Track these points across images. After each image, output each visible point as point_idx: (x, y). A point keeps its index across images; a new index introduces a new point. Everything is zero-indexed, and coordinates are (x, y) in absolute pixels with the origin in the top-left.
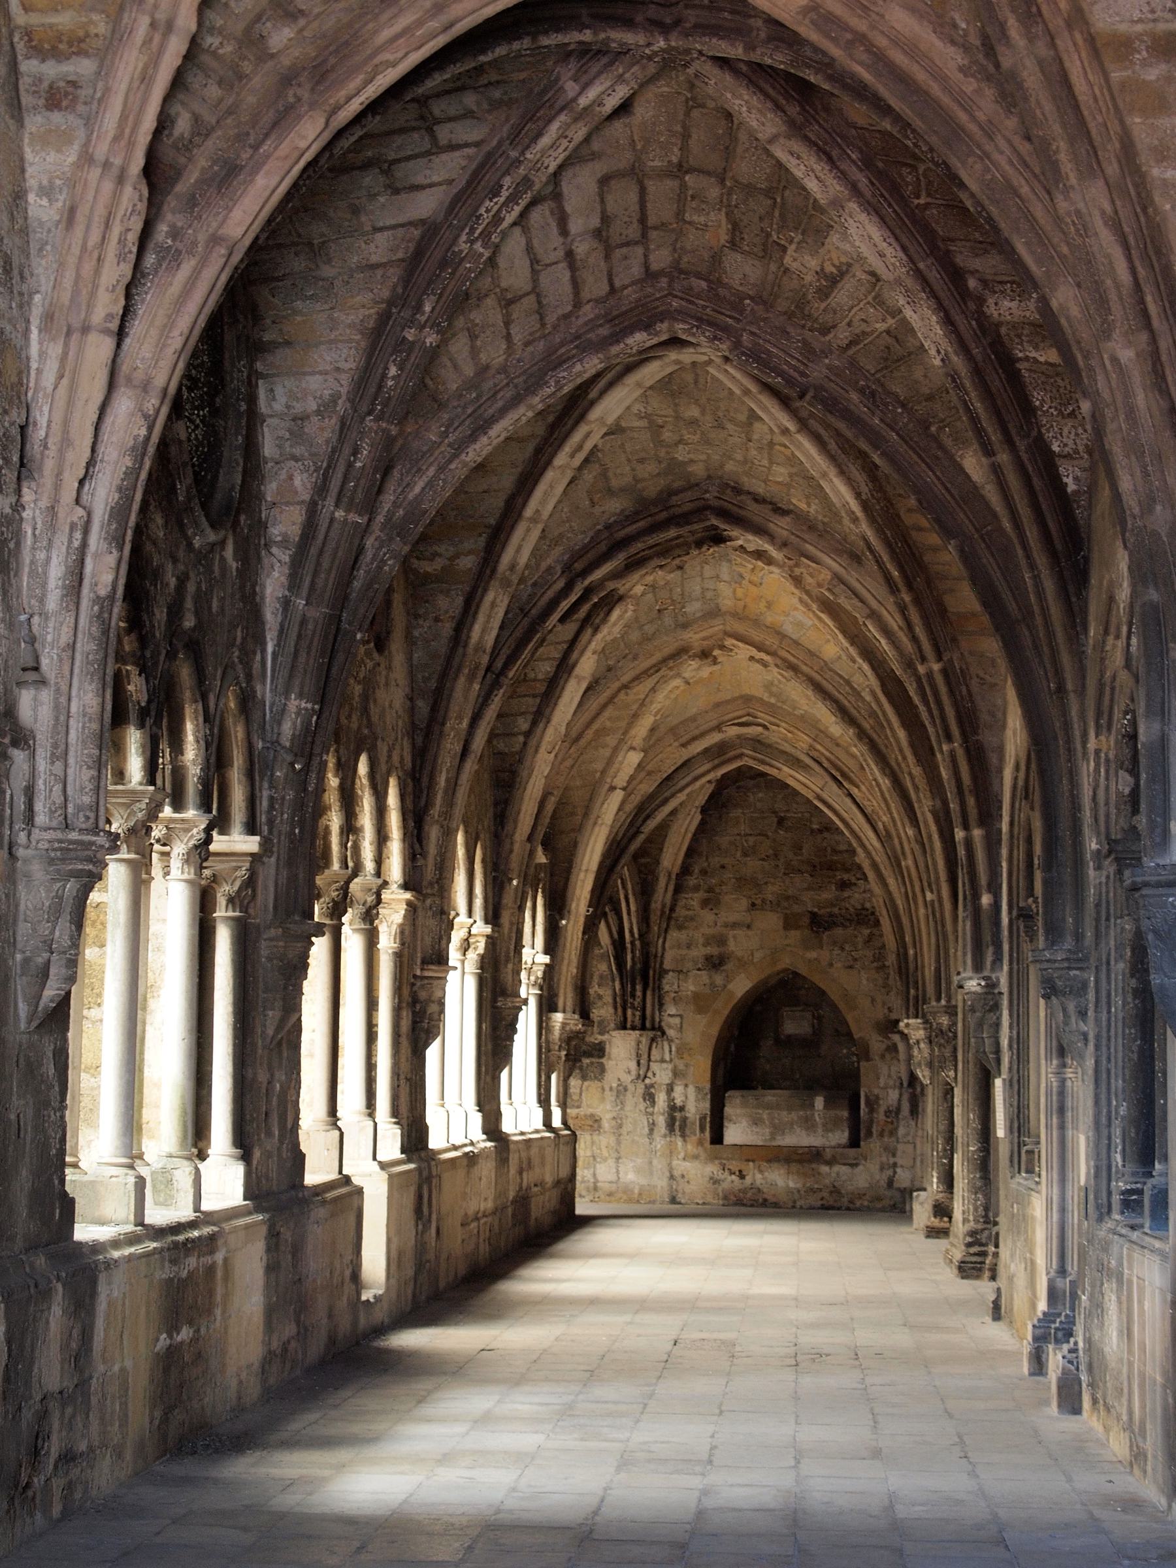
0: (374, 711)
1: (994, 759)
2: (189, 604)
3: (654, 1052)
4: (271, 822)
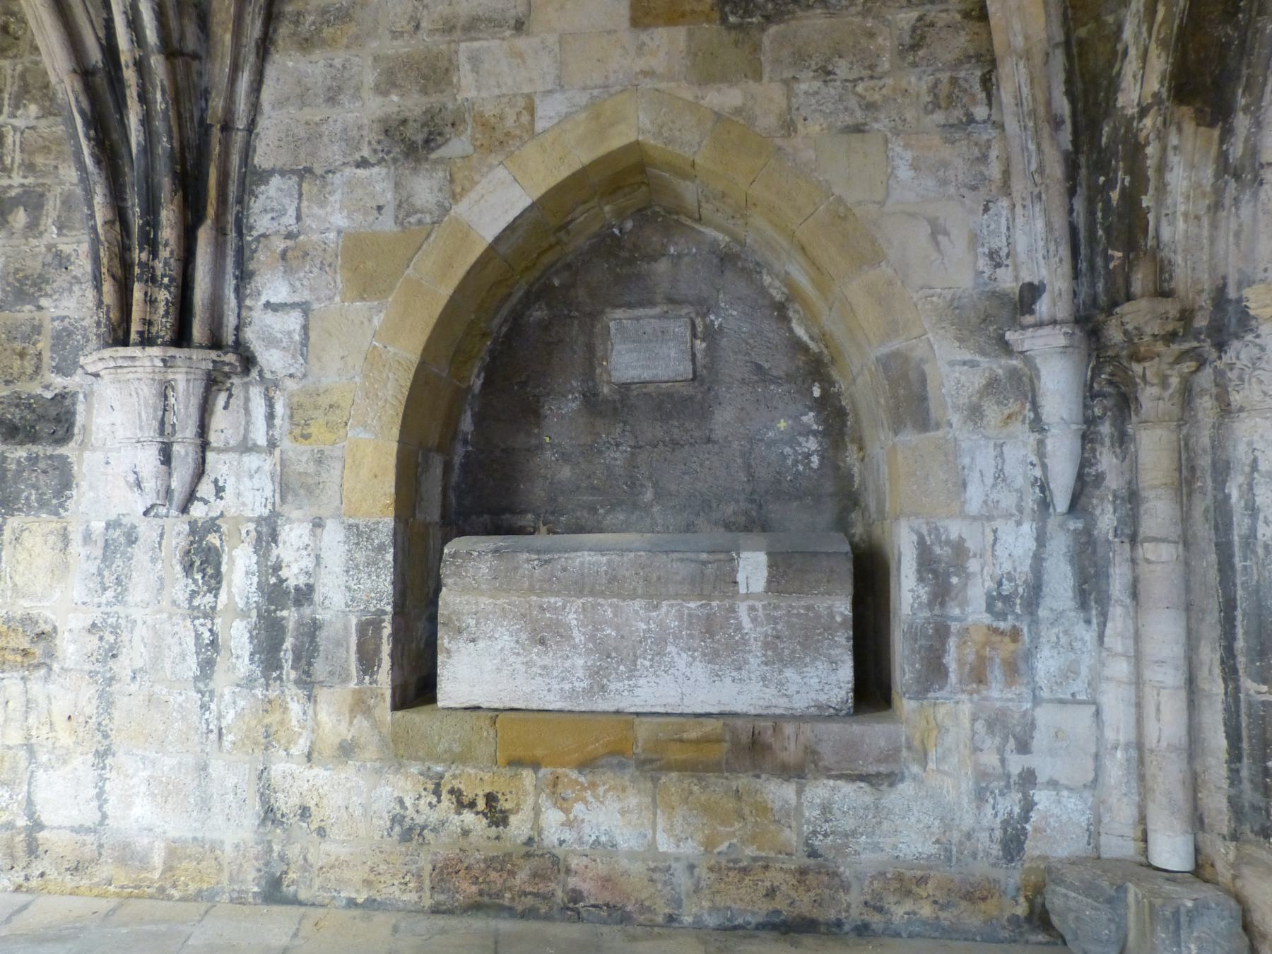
3: (223, 424)
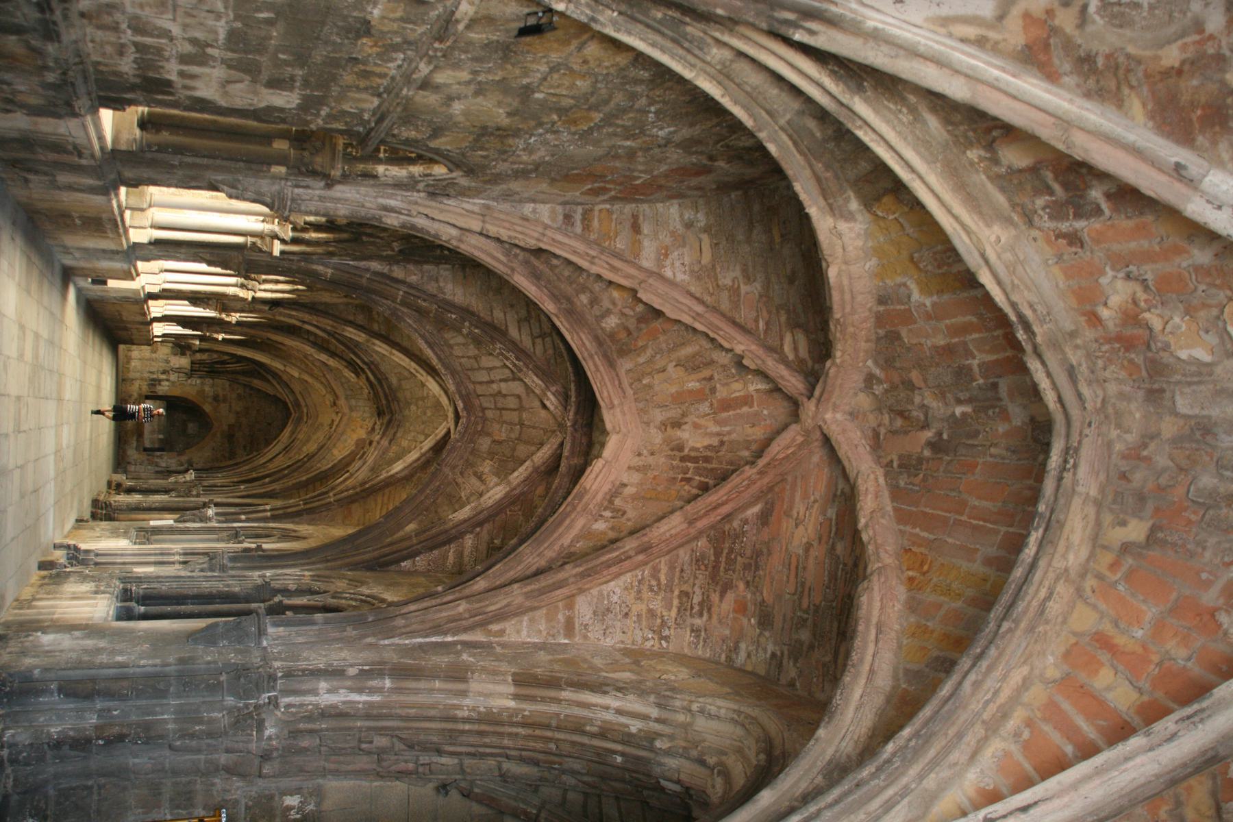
0: (323, 293)
1: (297, 520)
2: (372, 240)
4: (284, 259)
